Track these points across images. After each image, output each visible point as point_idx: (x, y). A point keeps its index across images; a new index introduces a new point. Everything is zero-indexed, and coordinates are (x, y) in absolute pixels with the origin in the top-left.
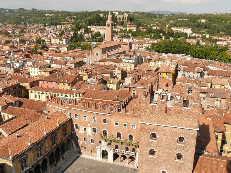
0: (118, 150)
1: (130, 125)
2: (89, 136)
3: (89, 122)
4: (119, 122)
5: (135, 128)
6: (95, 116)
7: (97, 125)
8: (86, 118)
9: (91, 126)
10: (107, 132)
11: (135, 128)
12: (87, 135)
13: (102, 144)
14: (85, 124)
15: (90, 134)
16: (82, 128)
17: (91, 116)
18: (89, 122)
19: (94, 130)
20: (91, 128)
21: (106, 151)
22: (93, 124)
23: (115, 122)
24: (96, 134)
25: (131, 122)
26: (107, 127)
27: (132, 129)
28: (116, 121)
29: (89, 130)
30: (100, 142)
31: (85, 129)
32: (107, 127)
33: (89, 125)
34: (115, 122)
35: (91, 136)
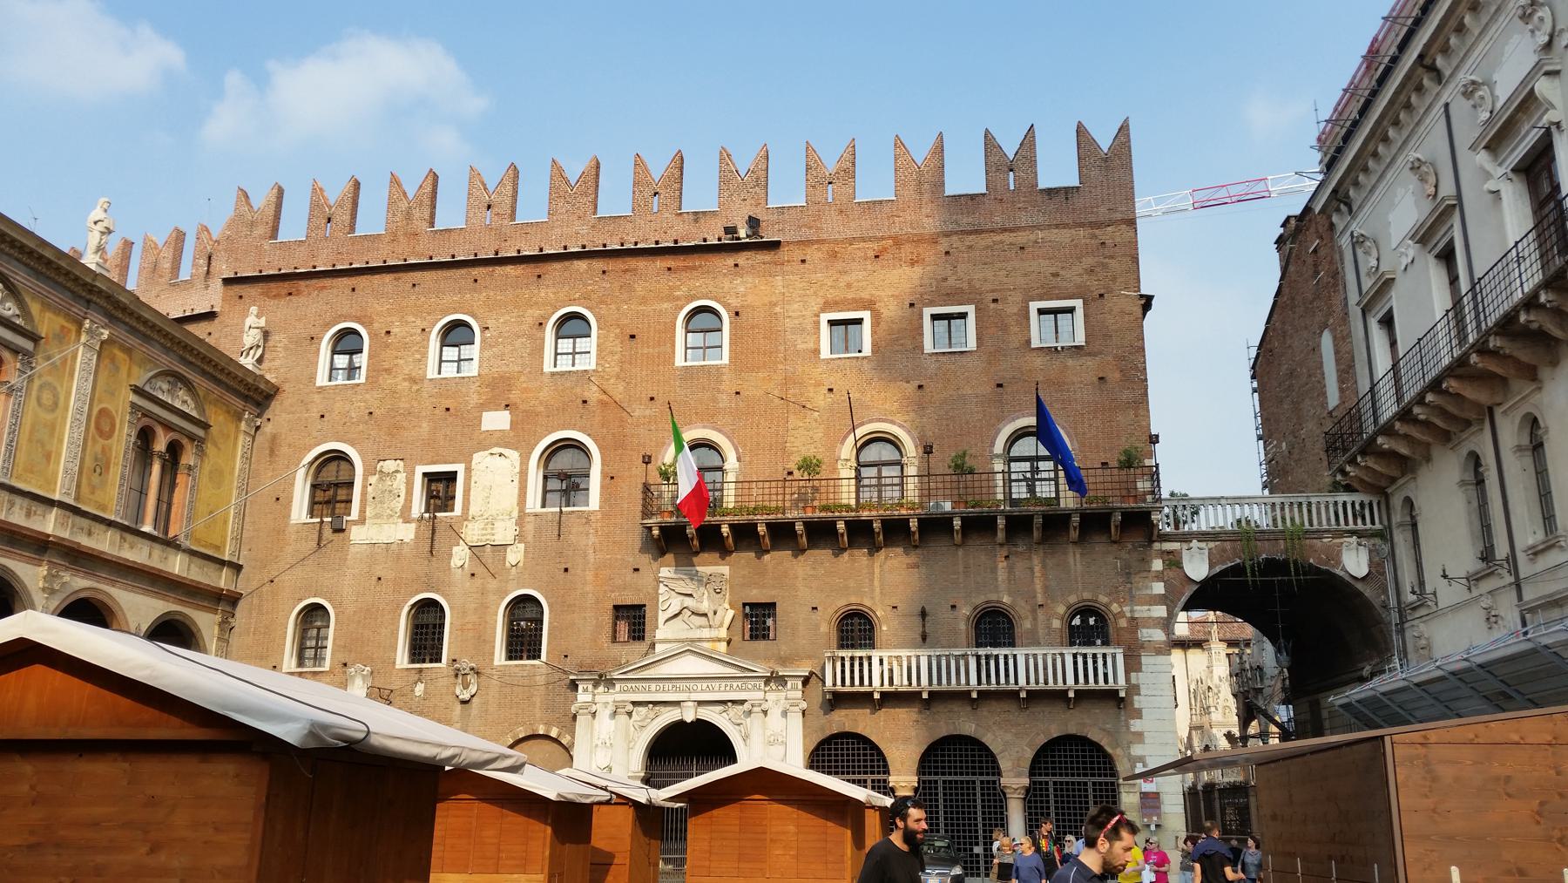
0: (876, 655)
1: (1012, 309)
2: (486, 556)
3: (498, 391)
4: (868, 305)
5: (1080, 339)
6: (585, 299)
7: (611, 404)
8: (473, 351)
9: (518, 439)
10: (731, 463)
11: (1080, 339)
12: (460, 555)
13: (659, 635)
14: (455, 415)
15: (504, 532)
16: (401, 477)
17: (530, 304)
18: (498, 391)
19: (565, 482)
20: (514, 455)
21: (701, 724)
22: (544, 394)
23: (825, 318)
24: (587, 518)
25: (1021, 281)
26: (724, 400)
27: (1039, 361)
28: (828, 306)
29: (499, 489)
30: (633, 620)
31: (441, 488)
32: (724, 400)
33: (495, 420)
34: (825, 318)
35: (515, 555)
